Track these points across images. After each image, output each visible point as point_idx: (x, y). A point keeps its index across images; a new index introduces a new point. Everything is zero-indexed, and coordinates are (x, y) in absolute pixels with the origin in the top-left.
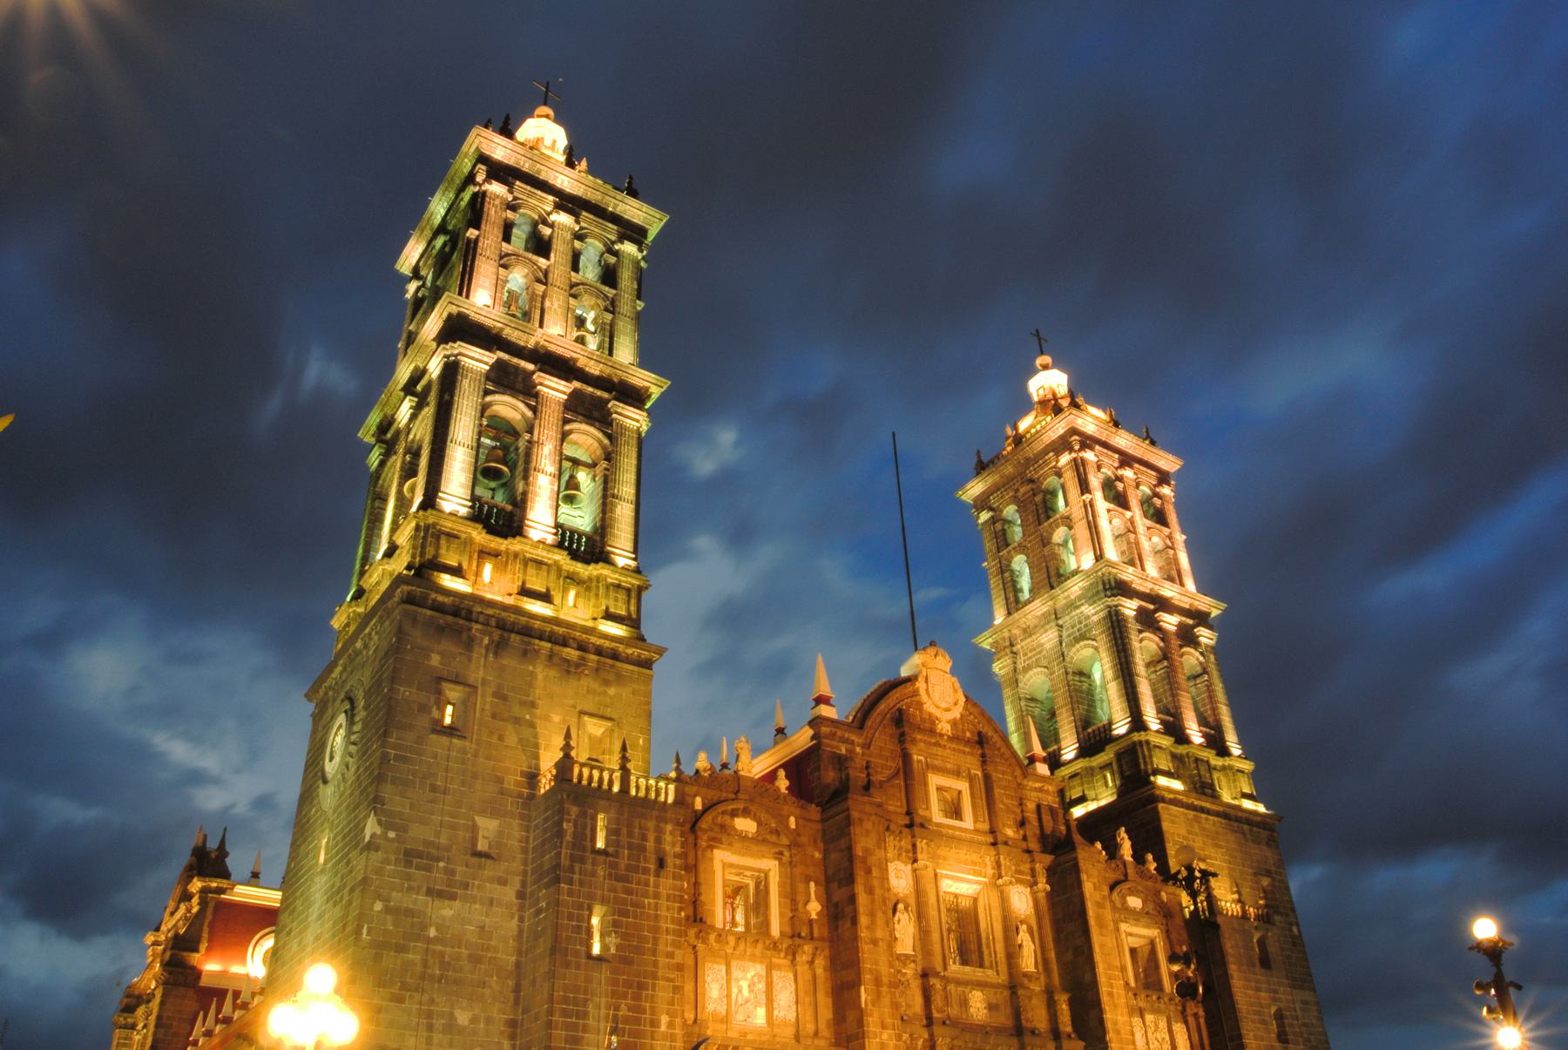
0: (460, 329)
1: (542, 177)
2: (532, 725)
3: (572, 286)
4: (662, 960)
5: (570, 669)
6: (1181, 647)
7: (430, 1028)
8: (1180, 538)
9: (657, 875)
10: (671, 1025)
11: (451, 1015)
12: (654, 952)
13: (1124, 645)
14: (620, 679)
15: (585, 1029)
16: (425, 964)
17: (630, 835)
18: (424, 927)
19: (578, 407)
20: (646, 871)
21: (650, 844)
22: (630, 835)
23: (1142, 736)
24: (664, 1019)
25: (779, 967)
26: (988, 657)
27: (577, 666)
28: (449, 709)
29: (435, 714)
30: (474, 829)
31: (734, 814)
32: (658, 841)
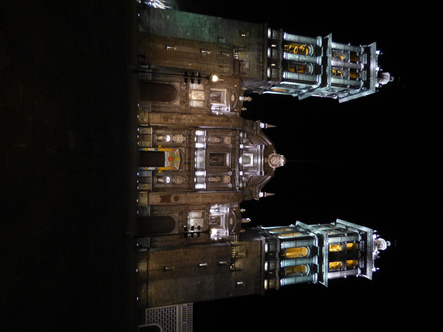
0: (325, 42)
1: (371, 61)
2: (245, 51)
3: (347, 68)
4: (202, 65)
5: (258, 60)
6: (309, 264)
7: (186, 28)
8: (345, 274)
9: (219, 66)
10: (190, 66)
11: (188, 32)
12: (203, 64)
13: (304, 239)
14: (259, 72)
15: (188, 47)
16: (197, 27)
17: (225, 60)
18: (203, 27)
19: (317, 67)
20: (219, 63)
21: (224, 65)
22: (225, 60)
23: (279, 241)
24: (191, 65)
25: (204, 103)
26: (294, 224)
27: (259, 61)
28: (244, 35)
29: (243, 30)
30: (222, 38)
31: (235, 95)
32: (225, 67)
